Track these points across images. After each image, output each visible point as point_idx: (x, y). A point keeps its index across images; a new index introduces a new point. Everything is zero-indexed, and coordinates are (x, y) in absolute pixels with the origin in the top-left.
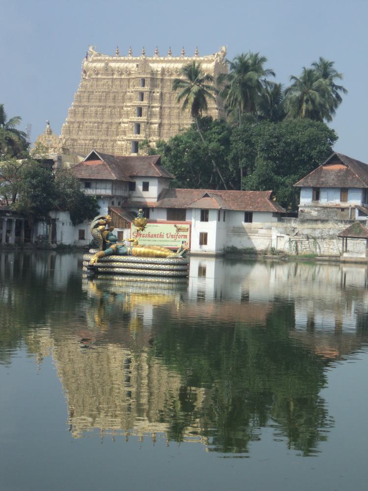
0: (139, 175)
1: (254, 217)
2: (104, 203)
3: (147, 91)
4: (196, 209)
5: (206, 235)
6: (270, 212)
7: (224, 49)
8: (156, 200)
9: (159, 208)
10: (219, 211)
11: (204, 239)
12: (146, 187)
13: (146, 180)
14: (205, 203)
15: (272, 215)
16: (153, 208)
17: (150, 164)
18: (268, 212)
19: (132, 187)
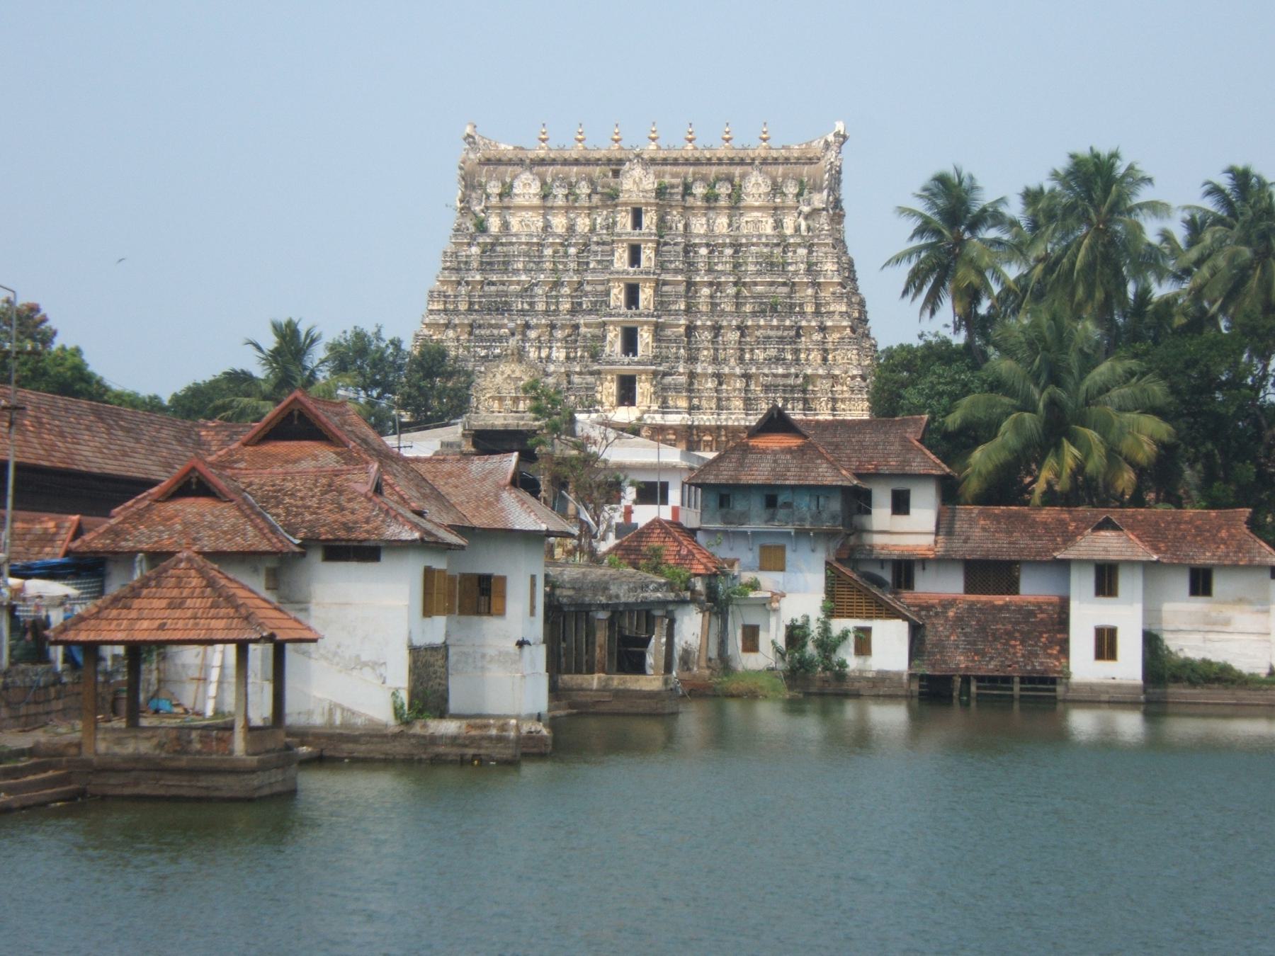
0: (884, 470)
1: (1219, 584)
2: (813, 551)
3: (651, 241)
4: (1082, 562)
5: (1112, 632)
6: (1261, 567)
7: (840, 127)
8: (932, 537)
9: (942, 561)
10: (1147, 566)
11: (1106, 644)
12: (901, 505)
13: (901, 485)
14: (1108, 545)
15: (1267, 575)
16: (924, 562)
17: (905, 440)
18: (1251, 567)
19: (858, 501)
